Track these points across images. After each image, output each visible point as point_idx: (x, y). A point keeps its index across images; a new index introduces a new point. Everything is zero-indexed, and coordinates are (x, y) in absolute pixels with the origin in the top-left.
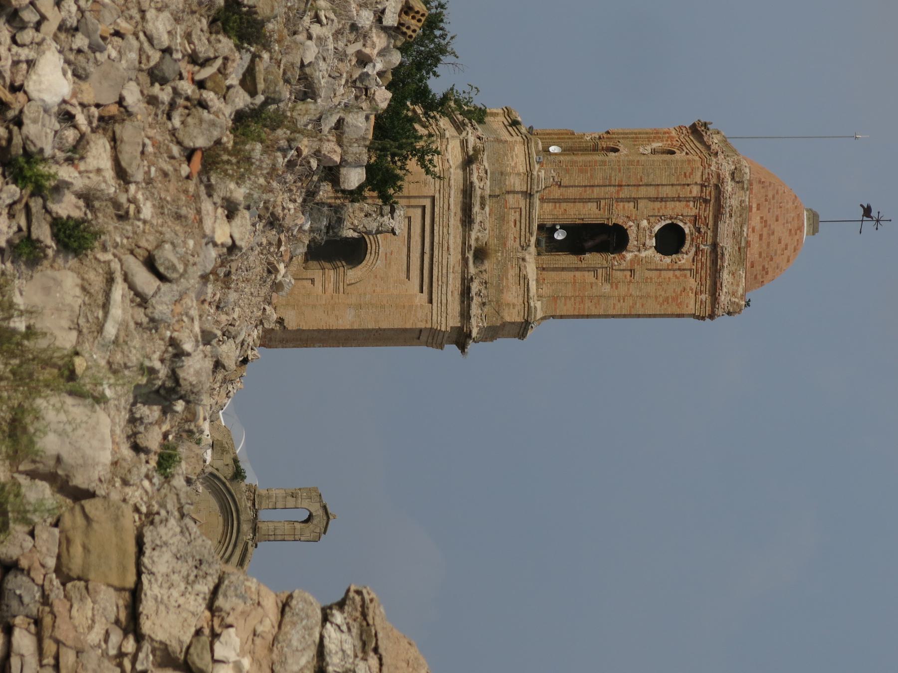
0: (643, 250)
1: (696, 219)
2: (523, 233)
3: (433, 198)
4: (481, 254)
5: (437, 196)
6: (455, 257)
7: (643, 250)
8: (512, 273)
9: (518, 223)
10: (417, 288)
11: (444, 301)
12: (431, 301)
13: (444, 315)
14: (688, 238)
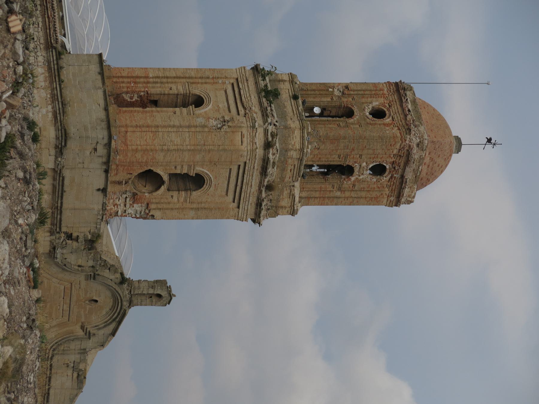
1: (393, 163)
2: (295, 175)
4: (270, 188)
5: (248, 162)
6: (255, 188)
8: (286, 193)
9: (292, 171)
11: (246, 208)
12: (239, 207)
13: (245, 215)
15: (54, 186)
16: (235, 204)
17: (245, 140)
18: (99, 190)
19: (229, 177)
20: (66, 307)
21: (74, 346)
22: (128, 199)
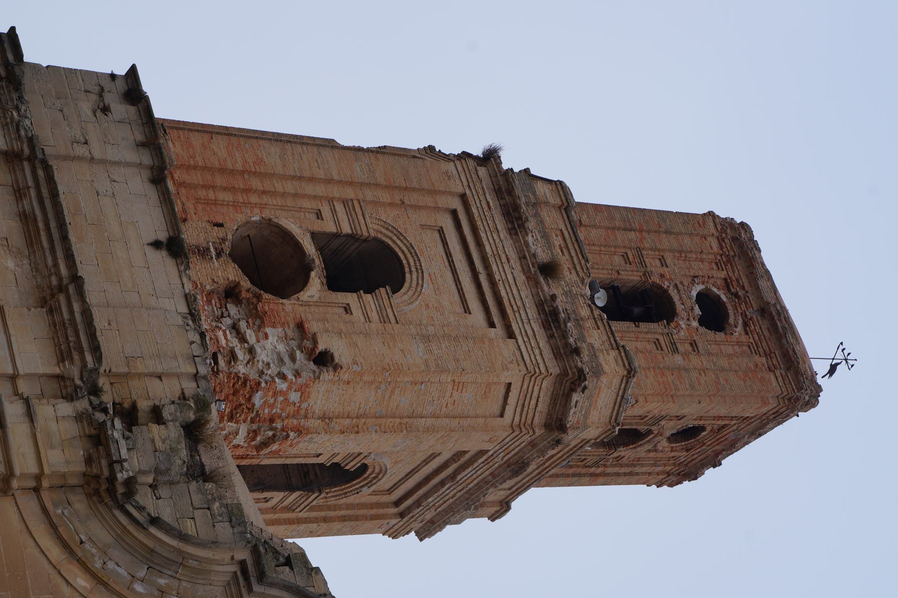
2: (576, 261)
3: (463, 197)
4: (549, 270)
5: (468, 192)
7: (688, 322)
9: (565, 251)
11: (530, 332)
12: (511, 335)
13: (537, 352)
14: (729, 307)
15: (26, 218)
18: (156, 244)
19: (449, 255)
22: (243, 325)
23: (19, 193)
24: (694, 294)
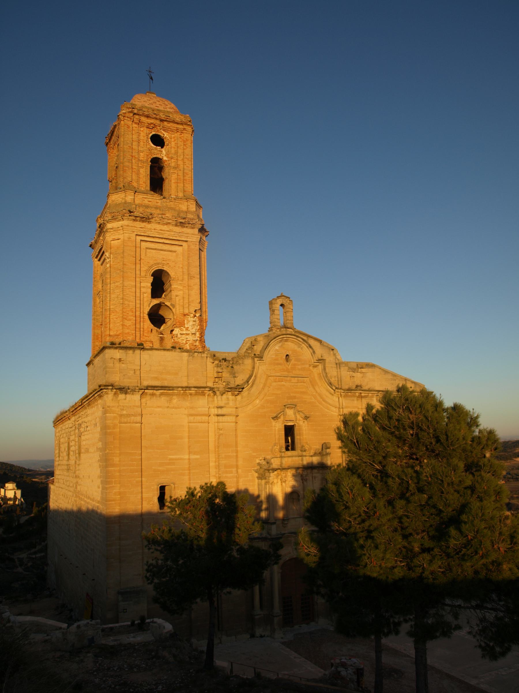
0: (163, 154)
10: (181, 248)
12: (186, 241)
14: (157, 133)
16: (184, 244)
17: (116, 237)
19: (156, 249)
20: (294, 380)
21: (332, 372)
23: (153, 395)
24: (153, 145)
